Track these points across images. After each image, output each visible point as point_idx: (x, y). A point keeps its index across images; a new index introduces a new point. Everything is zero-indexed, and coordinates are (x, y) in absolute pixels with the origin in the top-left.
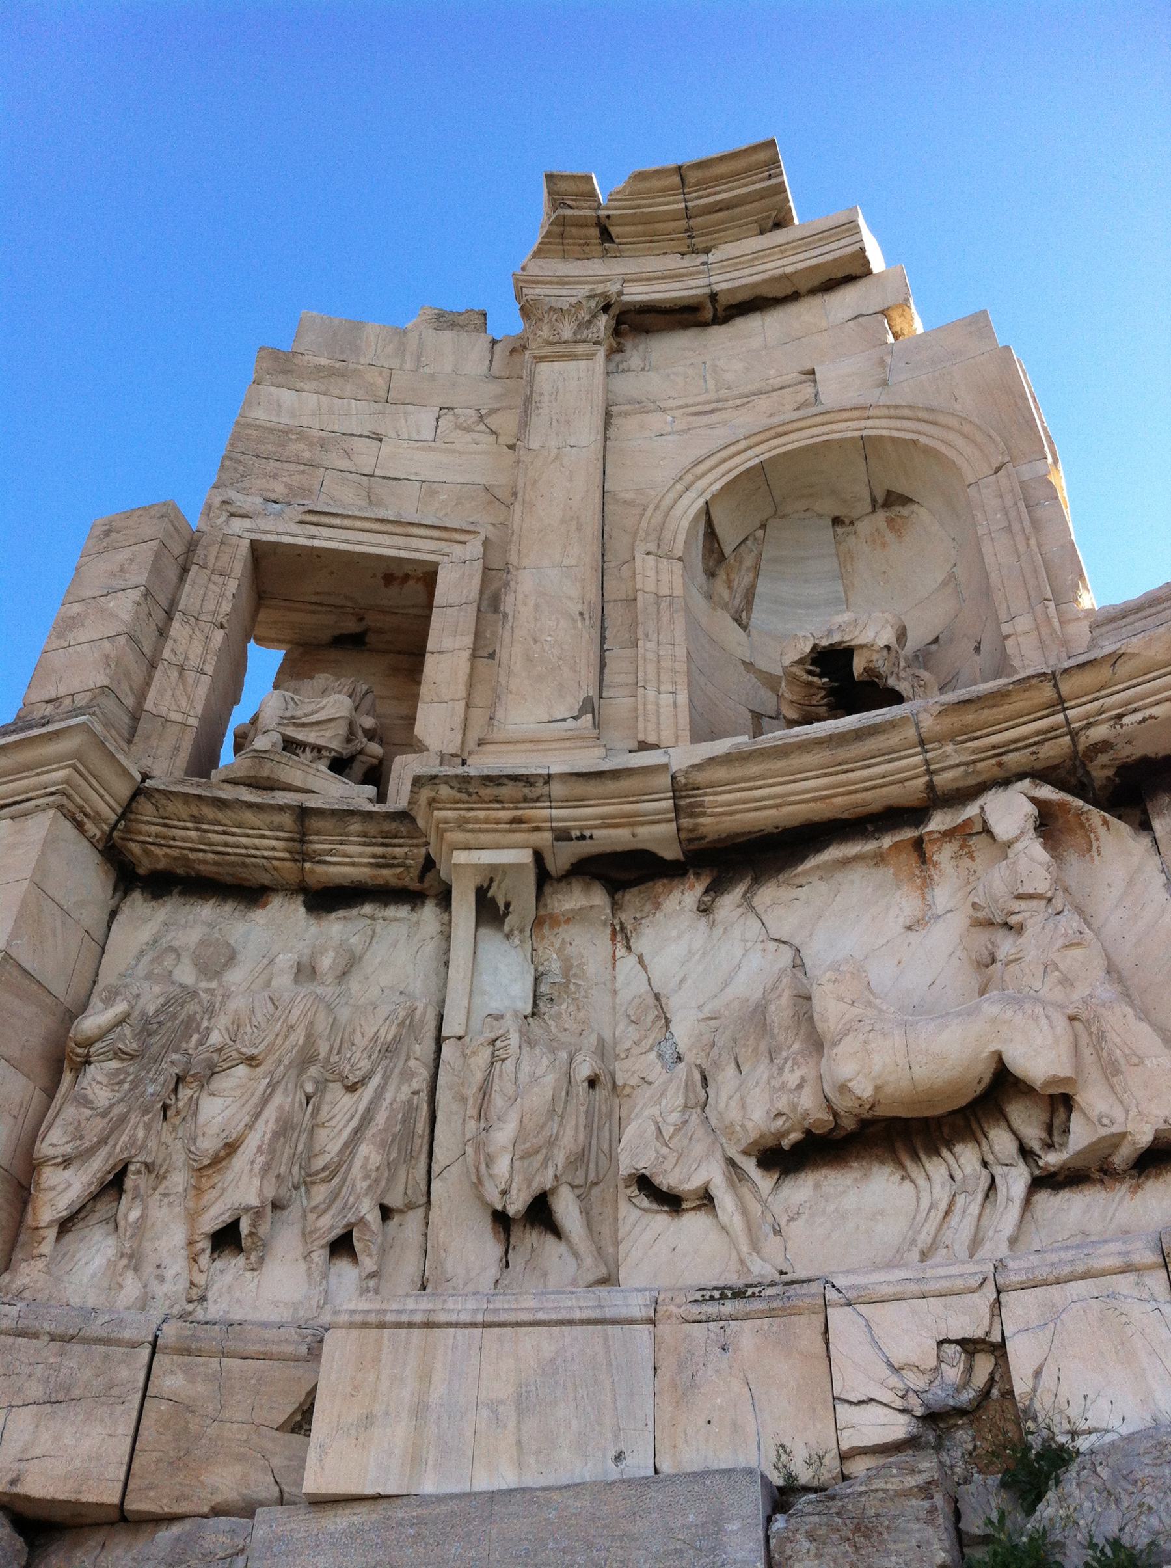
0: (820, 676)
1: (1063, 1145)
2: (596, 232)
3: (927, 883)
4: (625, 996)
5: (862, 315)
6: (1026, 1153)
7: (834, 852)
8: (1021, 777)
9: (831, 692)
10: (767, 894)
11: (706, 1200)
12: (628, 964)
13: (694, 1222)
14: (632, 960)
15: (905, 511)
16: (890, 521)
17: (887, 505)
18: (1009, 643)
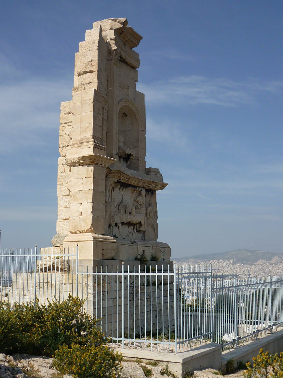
0: (127, 155)
1: (139, 229)
2: (121, 32)
3: (133, 194)
4: (113, 199)
5: (133, 79)
6: (136, 229)
7: (130, 188)
8: (144, 188)
9: (126, 157)
10: (124, 190)
11: (119, 227)
12: (113, 193)
13: (117, 228)
14: (113, 192)
15: (125, 117)
16: (122, 116)
17: (123, 114)
18: (140, 161)
